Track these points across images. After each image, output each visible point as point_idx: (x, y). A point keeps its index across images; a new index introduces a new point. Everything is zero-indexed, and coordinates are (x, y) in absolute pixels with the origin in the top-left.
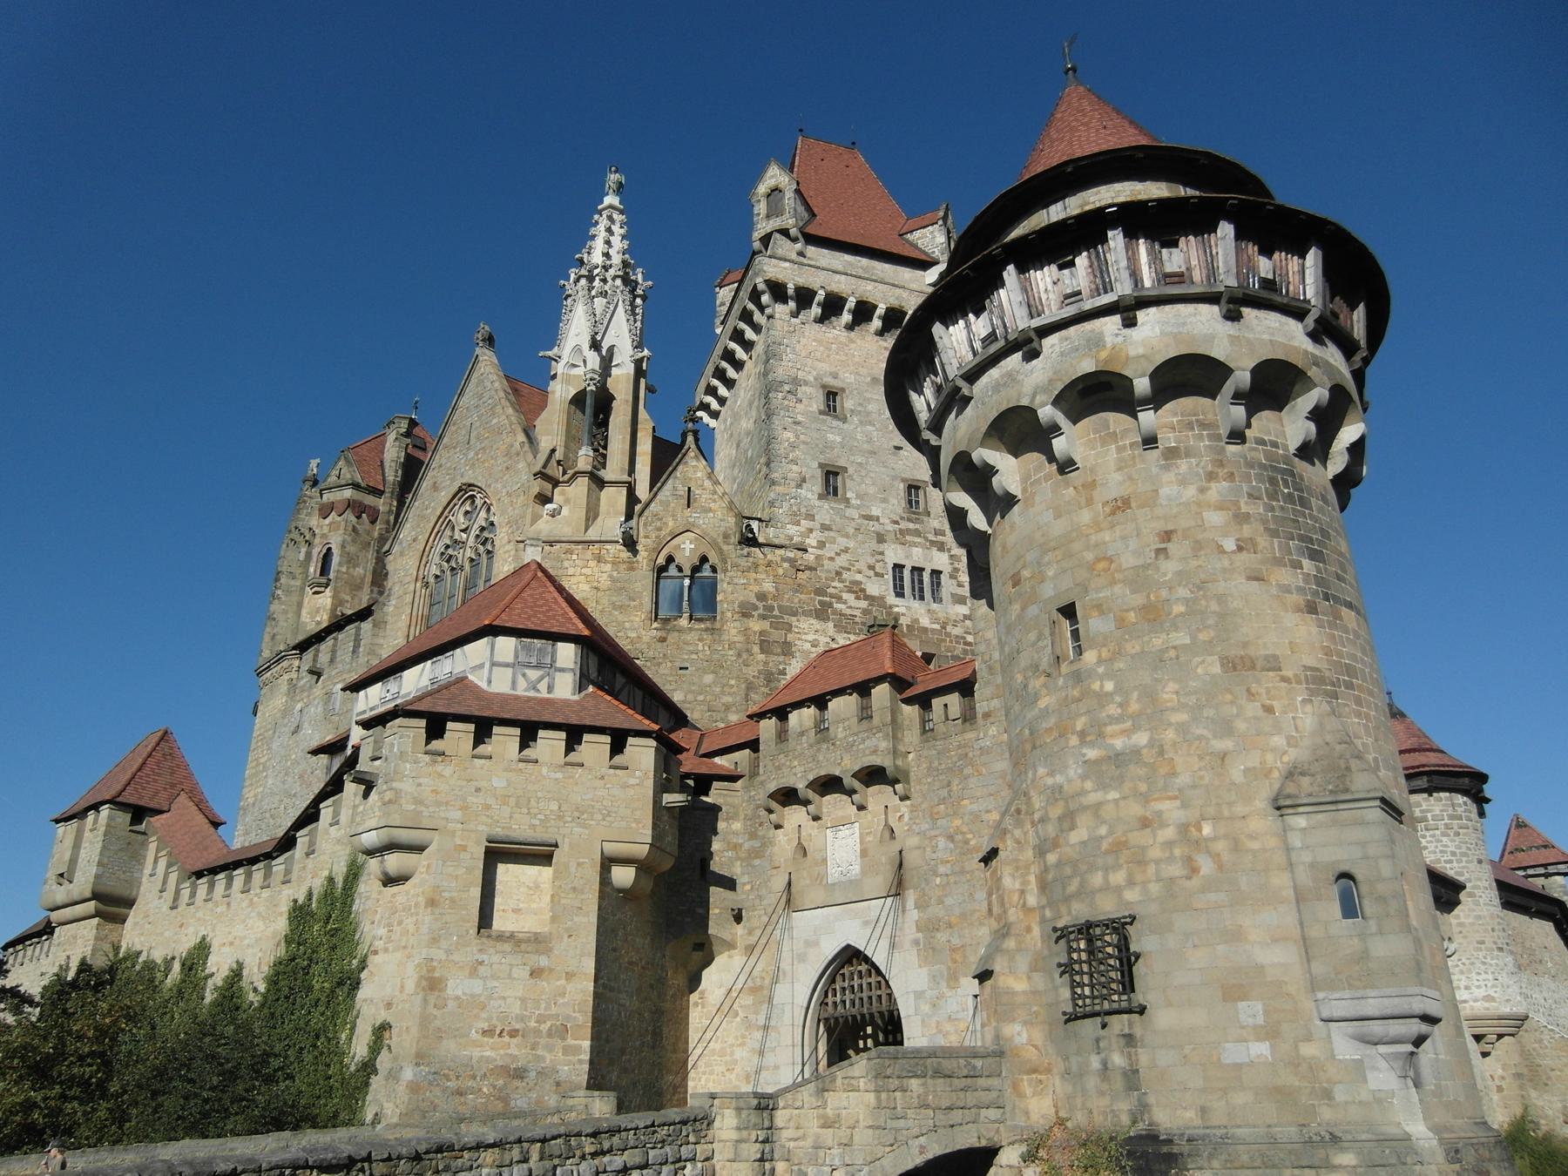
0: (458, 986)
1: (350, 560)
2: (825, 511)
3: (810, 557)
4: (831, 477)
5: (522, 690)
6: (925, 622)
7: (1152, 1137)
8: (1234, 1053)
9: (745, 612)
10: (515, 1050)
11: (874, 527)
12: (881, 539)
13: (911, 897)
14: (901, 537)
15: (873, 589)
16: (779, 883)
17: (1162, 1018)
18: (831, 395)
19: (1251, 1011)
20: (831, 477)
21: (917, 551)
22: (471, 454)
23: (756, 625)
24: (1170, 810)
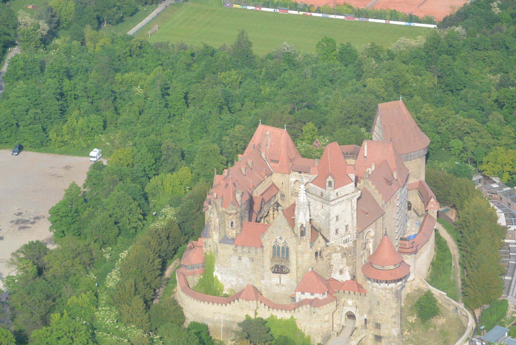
0: (324, 326)
1: (236, 223)
2: (336, 237)
3: (334, 245)
4: (337, 231)
5: (323, 298)
6: (347, 246)
7: (380, 336)
8: (386, 332)
9: (327, 256)
10: (328, 329)
11: (342, 236)
12: (342, 237)
13: (357, 309)
14: (345, 236)
15: (341, 246)
16: (342, 304)
17: (382, 330)
18: (337, 217)
19: (388, 330)
20: (337, 231)
21: (347, 237)
22: (281, 231)
23: (328, 257)
24: (384, 318)
